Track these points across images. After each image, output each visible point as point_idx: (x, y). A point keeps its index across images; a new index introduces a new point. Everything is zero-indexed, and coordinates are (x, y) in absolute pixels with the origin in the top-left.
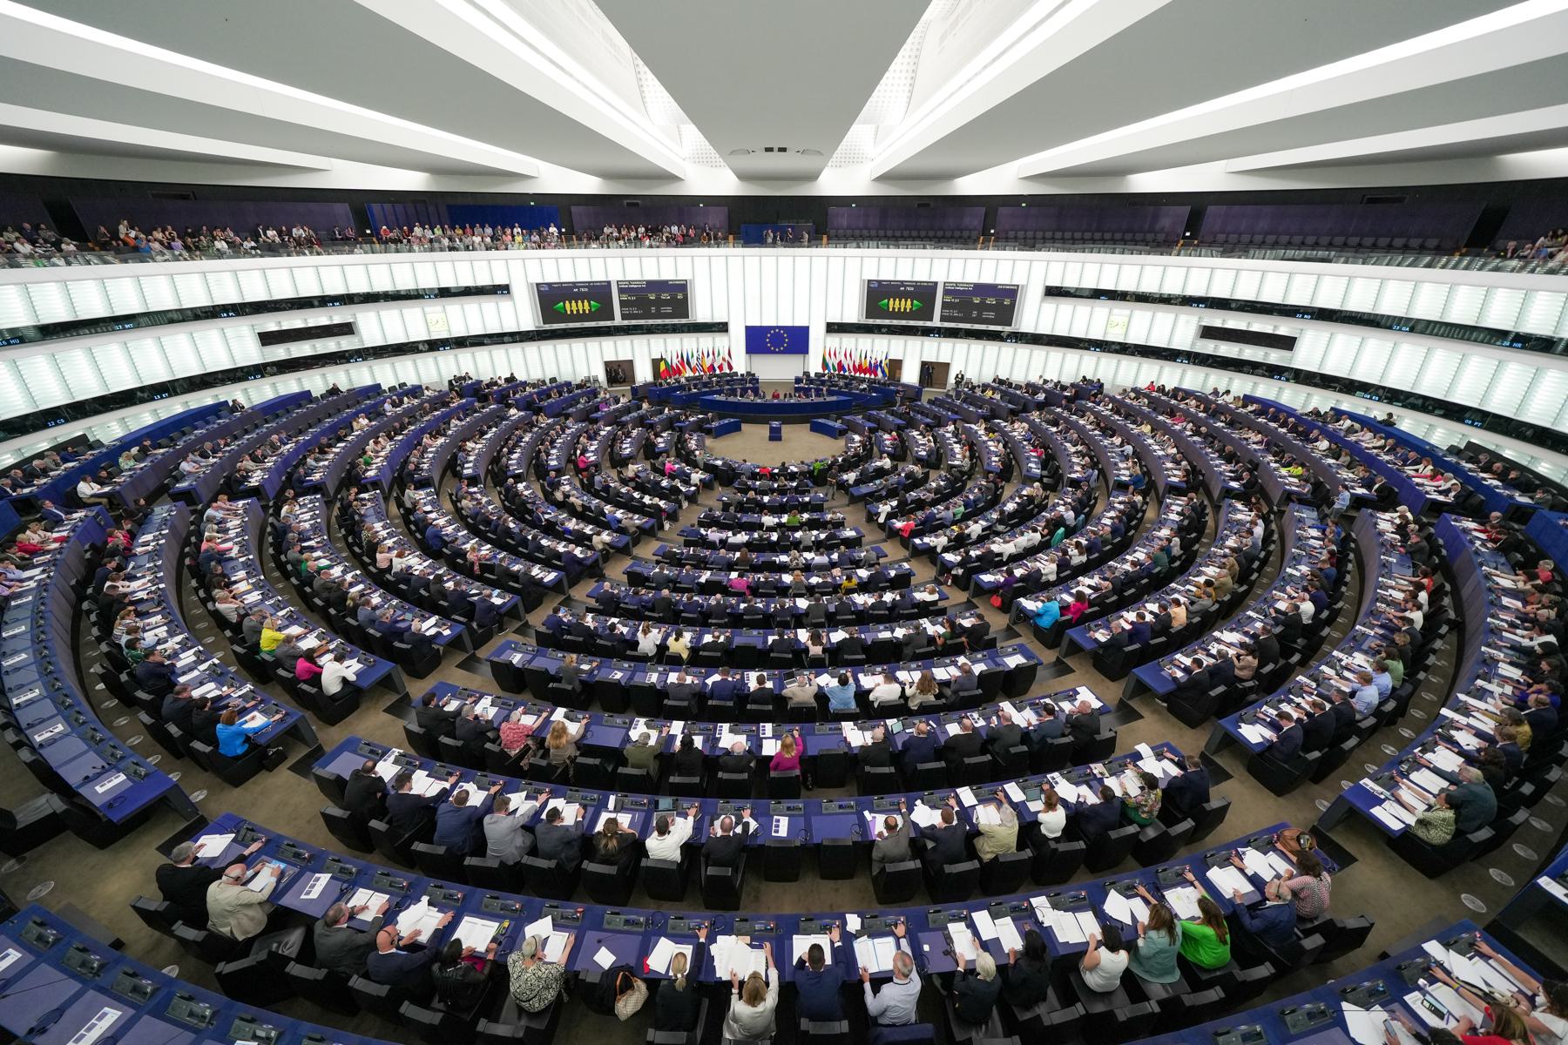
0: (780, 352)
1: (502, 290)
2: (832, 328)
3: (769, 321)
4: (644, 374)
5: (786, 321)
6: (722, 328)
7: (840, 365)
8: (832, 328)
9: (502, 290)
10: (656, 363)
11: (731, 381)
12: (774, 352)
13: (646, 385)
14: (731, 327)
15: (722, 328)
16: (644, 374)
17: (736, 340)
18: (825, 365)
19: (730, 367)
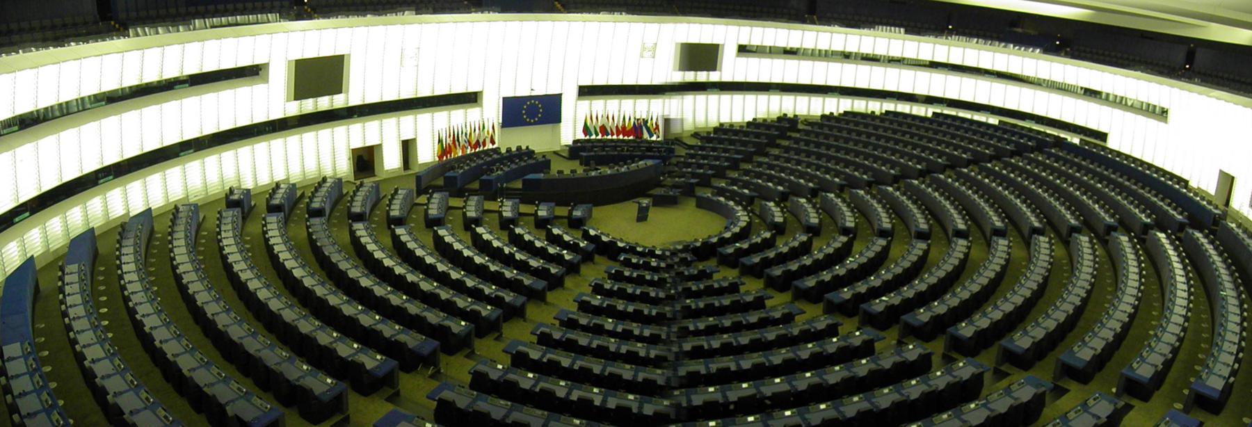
0: (536, 123)
1: (252, 72)
2: (587, 92)
3: (523, 92)
4: (391, 160)
5: (540, 91)
6: (470, 99)
7: (604, 130)
8: (587, 92)
9: (252, 72)
10: (408, 147)
11: (495, 159)
12: (530, 124)
13: (393, 171)
14: (486, 99)
15: (470, 99)
16: (391, 160)
17: (490, 113)
18: (586, 130)
19: (493, 142)
